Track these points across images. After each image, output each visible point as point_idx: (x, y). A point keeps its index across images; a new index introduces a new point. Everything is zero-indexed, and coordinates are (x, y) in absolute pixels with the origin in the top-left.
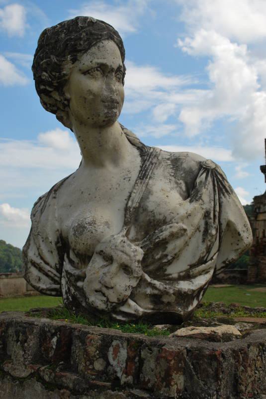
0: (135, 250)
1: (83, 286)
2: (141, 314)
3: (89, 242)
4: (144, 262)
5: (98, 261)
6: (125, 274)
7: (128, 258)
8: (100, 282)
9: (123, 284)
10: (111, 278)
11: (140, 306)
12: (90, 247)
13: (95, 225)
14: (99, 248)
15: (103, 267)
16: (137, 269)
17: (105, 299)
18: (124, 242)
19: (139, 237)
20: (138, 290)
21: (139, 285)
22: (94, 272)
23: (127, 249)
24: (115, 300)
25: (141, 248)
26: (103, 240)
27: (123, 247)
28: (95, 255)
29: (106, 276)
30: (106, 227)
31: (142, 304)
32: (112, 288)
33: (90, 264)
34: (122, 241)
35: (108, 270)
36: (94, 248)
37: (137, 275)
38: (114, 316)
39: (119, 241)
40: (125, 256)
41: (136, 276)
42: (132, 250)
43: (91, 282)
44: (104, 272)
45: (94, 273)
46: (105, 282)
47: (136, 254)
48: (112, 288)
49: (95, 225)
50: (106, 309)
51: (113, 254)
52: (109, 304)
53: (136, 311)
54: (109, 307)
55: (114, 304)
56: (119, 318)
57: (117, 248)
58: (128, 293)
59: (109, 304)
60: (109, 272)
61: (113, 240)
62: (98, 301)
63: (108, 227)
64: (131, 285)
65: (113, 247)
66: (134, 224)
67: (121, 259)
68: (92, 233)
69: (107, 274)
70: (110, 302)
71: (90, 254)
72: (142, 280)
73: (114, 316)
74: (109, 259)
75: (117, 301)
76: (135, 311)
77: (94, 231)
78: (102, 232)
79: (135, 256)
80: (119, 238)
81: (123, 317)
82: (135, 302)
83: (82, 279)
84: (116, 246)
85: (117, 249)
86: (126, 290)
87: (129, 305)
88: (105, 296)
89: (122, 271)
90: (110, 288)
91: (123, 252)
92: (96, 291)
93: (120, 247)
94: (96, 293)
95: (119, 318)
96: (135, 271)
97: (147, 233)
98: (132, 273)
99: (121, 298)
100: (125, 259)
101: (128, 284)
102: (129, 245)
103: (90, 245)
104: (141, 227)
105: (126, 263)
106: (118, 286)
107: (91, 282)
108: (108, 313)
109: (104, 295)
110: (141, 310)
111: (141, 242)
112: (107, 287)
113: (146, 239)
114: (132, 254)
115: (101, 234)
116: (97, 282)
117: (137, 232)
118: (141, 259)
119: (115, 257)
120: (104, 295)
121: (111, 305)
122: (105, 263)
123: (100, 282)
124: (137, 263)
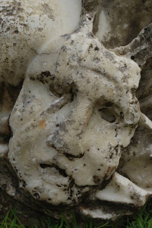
0: (123, 65)
1: (6, 154)
2: (143, 200)
3: (12, 53)
4: (140, 93)
5: (38, 96)
6: (104, 122)
7: (111, 85)
8: (53, 146)
9: (103, 142)
10: (78, 135)
11: (136, 183)
12: (14, 66)
13: (21, 14)
14: (36, 67)
15: (53, 109)
16: (132, 107)
17: (65, 181)
18: (97, 49)
19: (119, 35)
20: (131, 152)
21: (134, 142)
22: (32, 121)
23: (106, 64)
24: (89, 181)
25: (133, 58)
26: (44, 48)
27: (97, 59)
28: (27, 84)
29: (66, 131)
30: (46, 16)
31: (139, 178)
32: (81, 156)
33: (19, 104)
34: (91, 46)
35: (70, 115)
36: (24, 67)
37: (132, 119)
38: (86, 212)
39: (86, 47)
40: (104, 81)
41: (129, 122)
42: (117, 65)
43: (27, 146)
44: (59, 122)
45: (33, 126)
46: (65, 145)
47: (126, 73)
48: (81, 156)
49: (21, 14)
50: (69, 202)
51: (75, 78)
52: (75, 190)
53: (134, 196)
54: (75, 196)
55: (87, 189)
56: (97, 214)
57: (83, 63)
58: (115, 162)
59: (75, 190)
60: (71, 122)
61: (69, 46)
62: (51, 189)
63: (51, 17)
64: (120, 144)
65: (75, 63)
66: (105, 6)
67: (97, 88)
68: (17, 32)
69: (68, 127)
70: (77, 186)
71: (15, 82)
72: (139, 129)
73: (86, 212)
74: (68, 92)
75: (93, 183)
76: (132, 198)
77: (20, 29)
78: (40, 29)
79: (125, 79)
80: (84, 41)
81: (105, 211)
82: (125, 176)
83: (1, 139)
84: (80, 60)
85: (84, 67)
86: (111, 157)
87: (118, 187)
88: (65, 175)
89: (98, 115)
90: (77, 157)
91: (97, 71)
92: (43, 165)
93: (88, 61)
94: (42, 170)
95: (97, 214)
96: (128, 112)
97: (135, 27)
98: (122, 118)
99: (101, 174)
100: (105, 88)
101: (114, 144)
102: (108, 55)
103: (13, 62)
104: (121, 12)
105: (108, 96)
106: (94, 151)
107: (27, 146)
108: (74, 207)
109: (63, 172)
110: (143, 193)
111: (129, 46)
112: (70, 156)
113: (138, 38)
114: (119, 75)
115: (38, 32)
116: (44, 145)
117: (113, 25)
118: (137, 85)
119: (81, 85)
120: (63, 172)
121: (79, 193)
122: (58, 101)
123: (53, 146)
124: (130, 95)
